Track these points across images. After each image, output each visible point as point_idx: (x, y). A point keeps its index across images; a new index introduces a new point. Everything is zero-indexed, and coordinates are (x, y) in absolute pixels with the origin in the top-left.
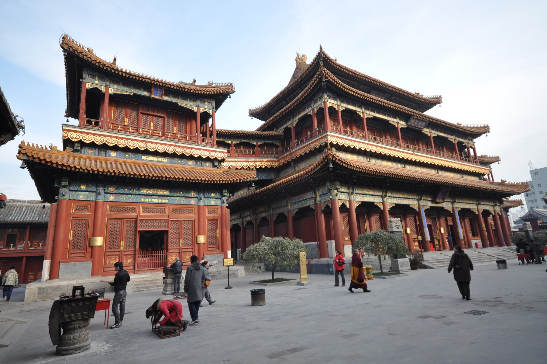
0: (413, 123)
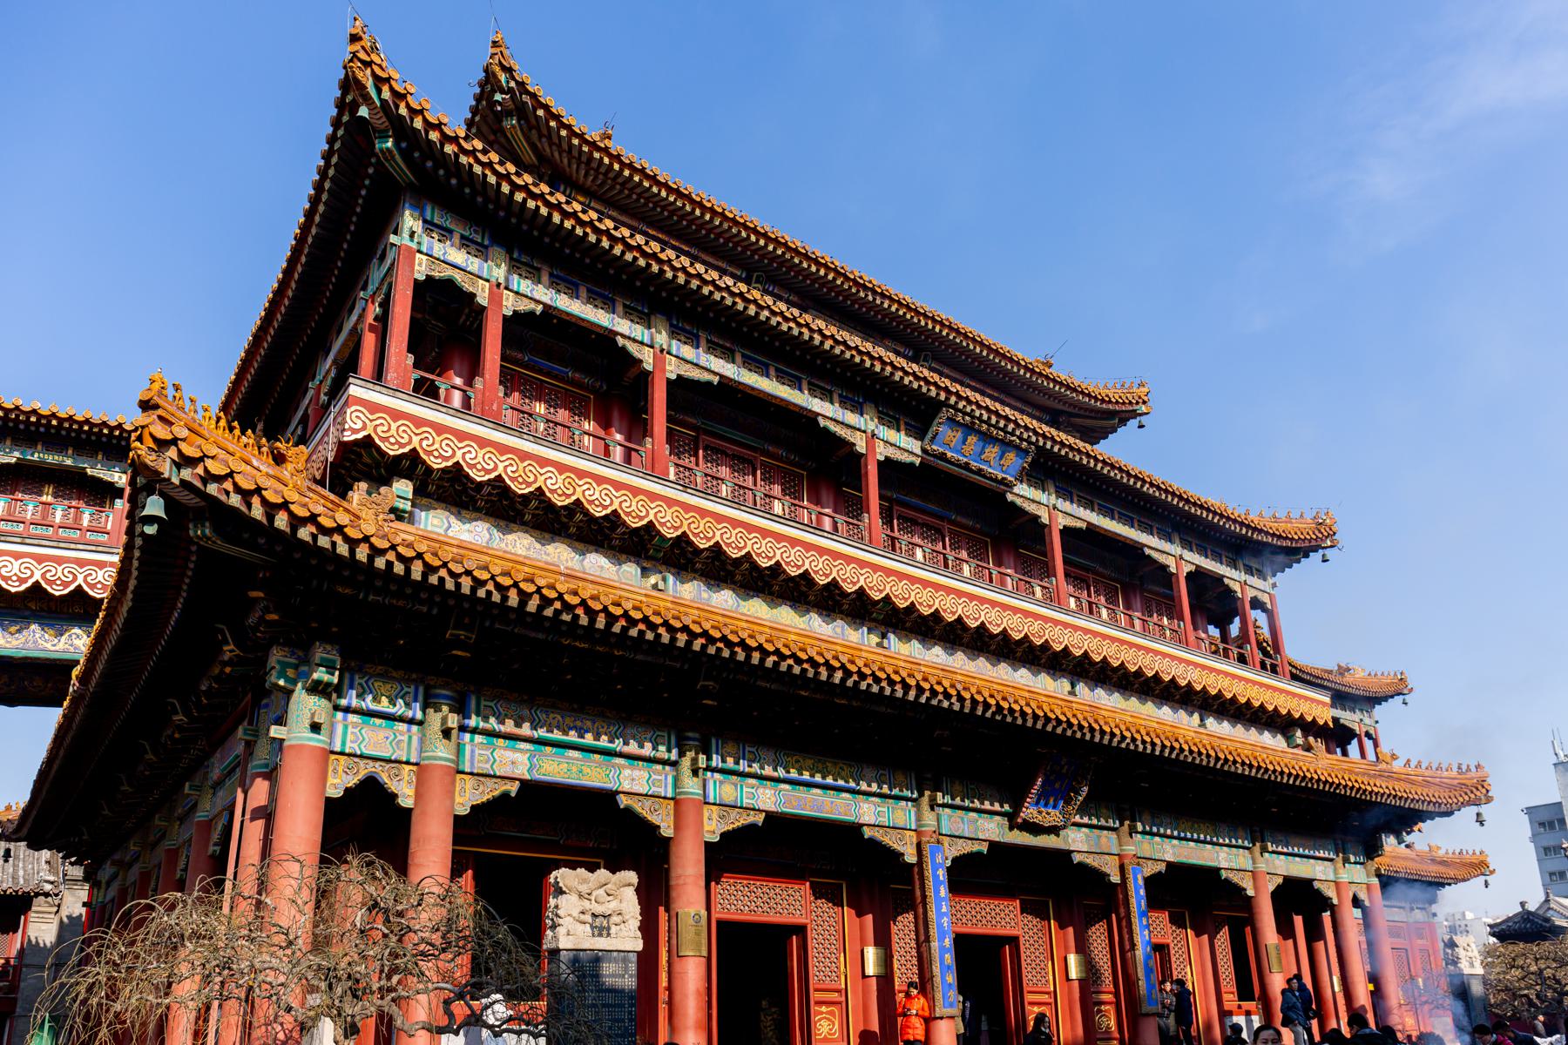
0: (951, 443)
